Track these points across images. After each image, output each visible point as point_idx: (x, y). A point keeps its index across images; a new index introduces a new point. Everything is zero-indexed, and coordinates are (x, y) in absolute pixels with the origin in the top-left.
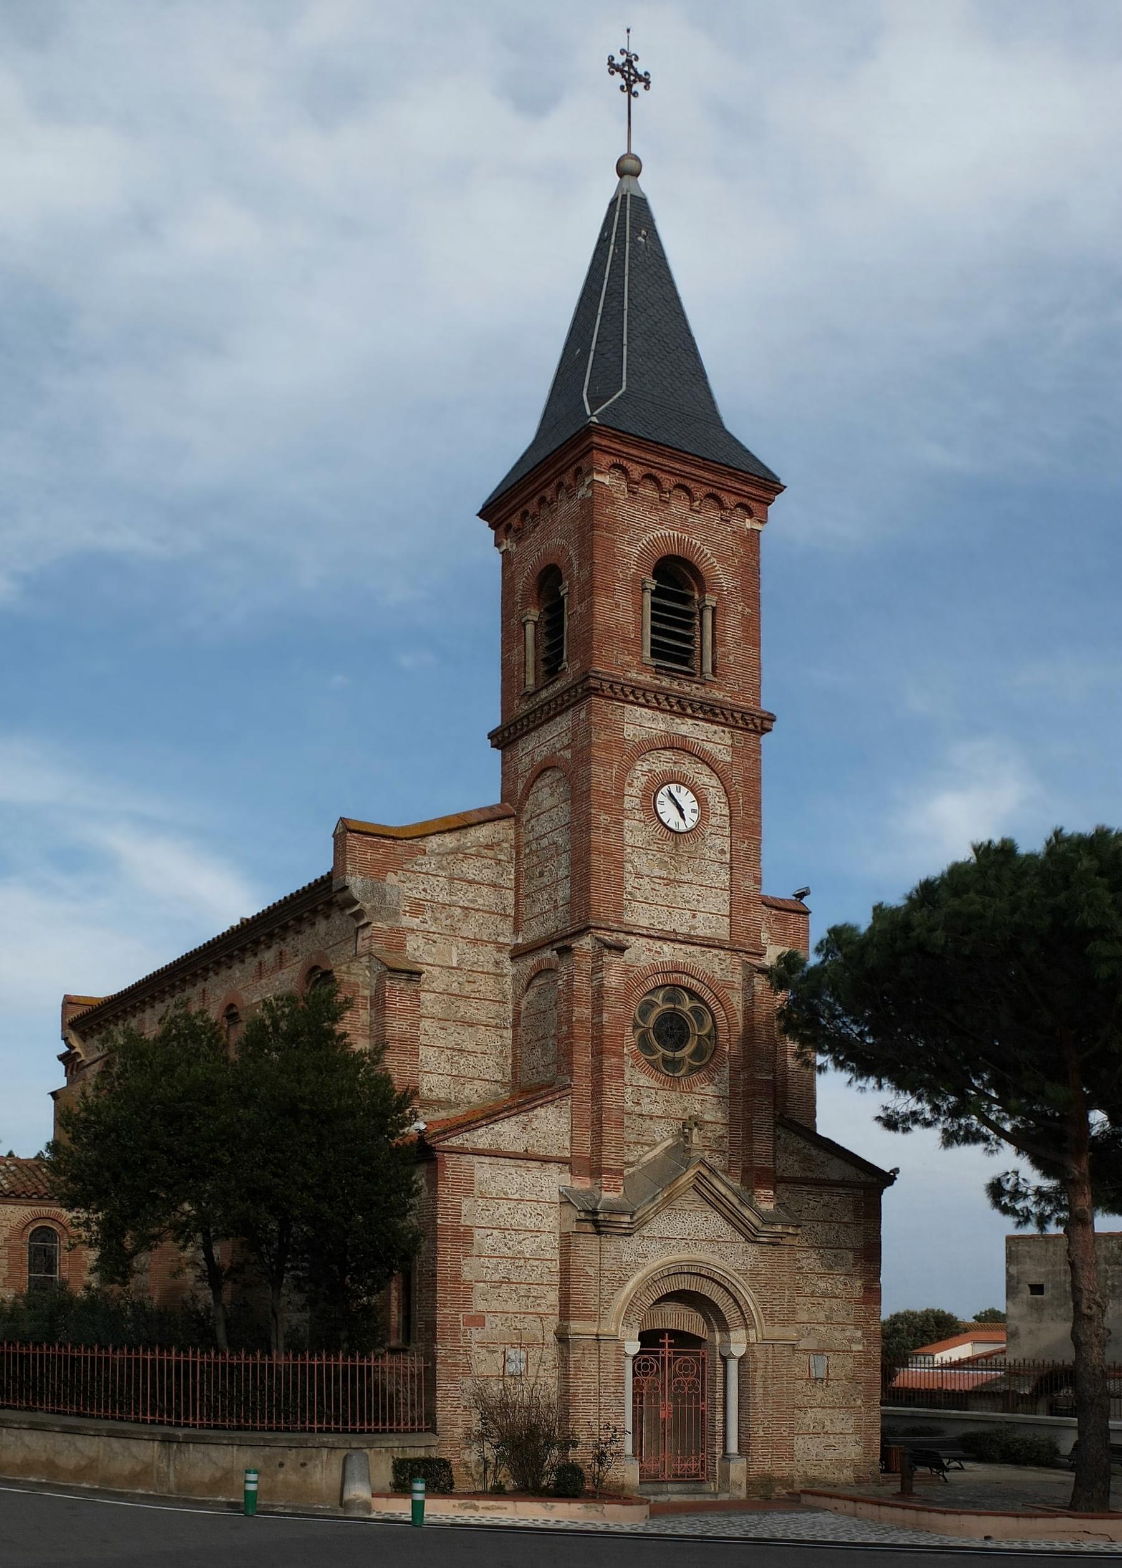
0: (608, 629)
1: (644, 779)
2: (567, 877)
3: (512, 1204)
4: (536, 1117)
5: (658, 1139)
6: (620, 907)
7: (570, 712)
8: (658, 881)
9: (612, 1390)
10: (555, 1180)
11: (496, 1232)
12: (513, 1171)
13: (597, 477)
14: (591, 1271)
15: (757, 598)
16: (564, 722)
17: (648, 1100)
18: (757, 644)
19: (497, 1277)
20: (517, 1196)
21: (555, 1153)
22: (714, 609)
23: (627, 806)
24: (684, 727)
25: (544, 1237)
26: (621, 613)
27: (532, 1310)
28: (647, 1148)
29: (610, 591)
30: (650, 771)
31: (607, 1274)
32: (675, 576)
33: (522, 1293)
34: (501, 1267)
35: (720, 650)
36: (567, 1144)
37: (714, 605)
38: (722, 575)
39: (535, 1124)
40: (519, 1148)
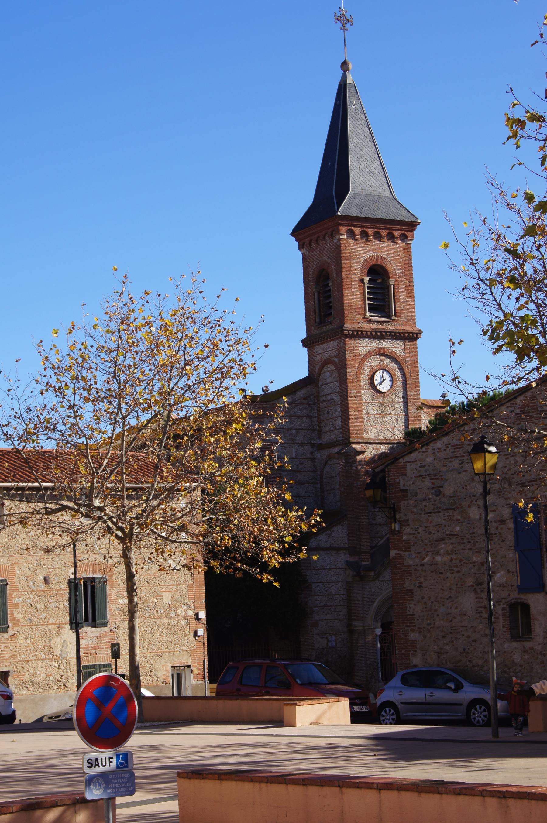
0: (350, 305)
1: (368, 370)
2: (339, 416)
3: (326, 571)
4: (334, 531)
5: (384, 534)
6: (362, 431)
7: (336, 341)
8: (377, 416)
9: (371, 651)
10: (342, 558)
11: (320, 584)
12: (326, 556)
13: (341, 237)
14: (360, 598)
15: (411, 276)
16: (333, 344)
17: (379, 517)
18: (413, 298)
19: (322, 604)
20: (328, 567)
21: (342, 545)
22: (394, 286)
23: (362, 384)
24: (385, 344)
25: (340, 584)
26: (355, 295)
27: (337, 618)
28: (379, 539)
29: (351, 288)
30: (371, 366)
31: (366, 599)
32: (377, 273)
33: (332, 610)
34: (324, 599)
35: (398, 304)
36: (347, 541)
37: (393, 283)
38: (395, 268)
39: (333, 534)
40: (327, 545)
